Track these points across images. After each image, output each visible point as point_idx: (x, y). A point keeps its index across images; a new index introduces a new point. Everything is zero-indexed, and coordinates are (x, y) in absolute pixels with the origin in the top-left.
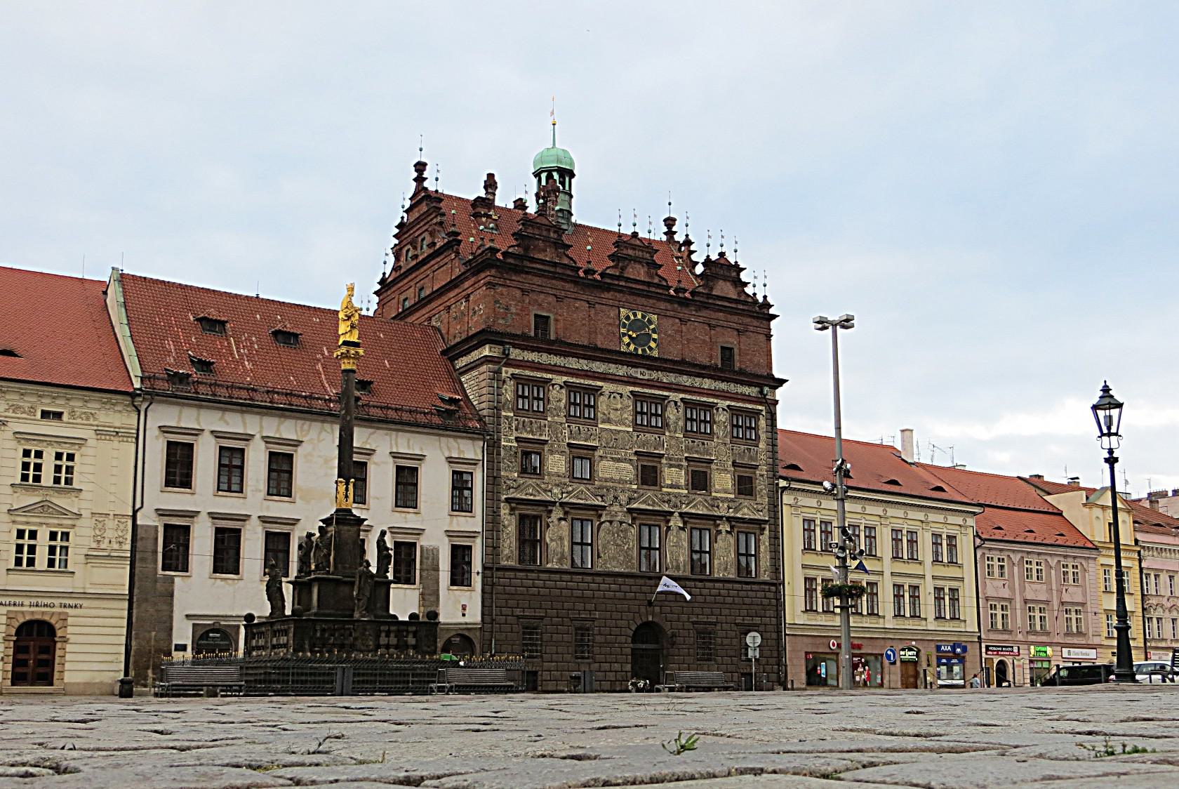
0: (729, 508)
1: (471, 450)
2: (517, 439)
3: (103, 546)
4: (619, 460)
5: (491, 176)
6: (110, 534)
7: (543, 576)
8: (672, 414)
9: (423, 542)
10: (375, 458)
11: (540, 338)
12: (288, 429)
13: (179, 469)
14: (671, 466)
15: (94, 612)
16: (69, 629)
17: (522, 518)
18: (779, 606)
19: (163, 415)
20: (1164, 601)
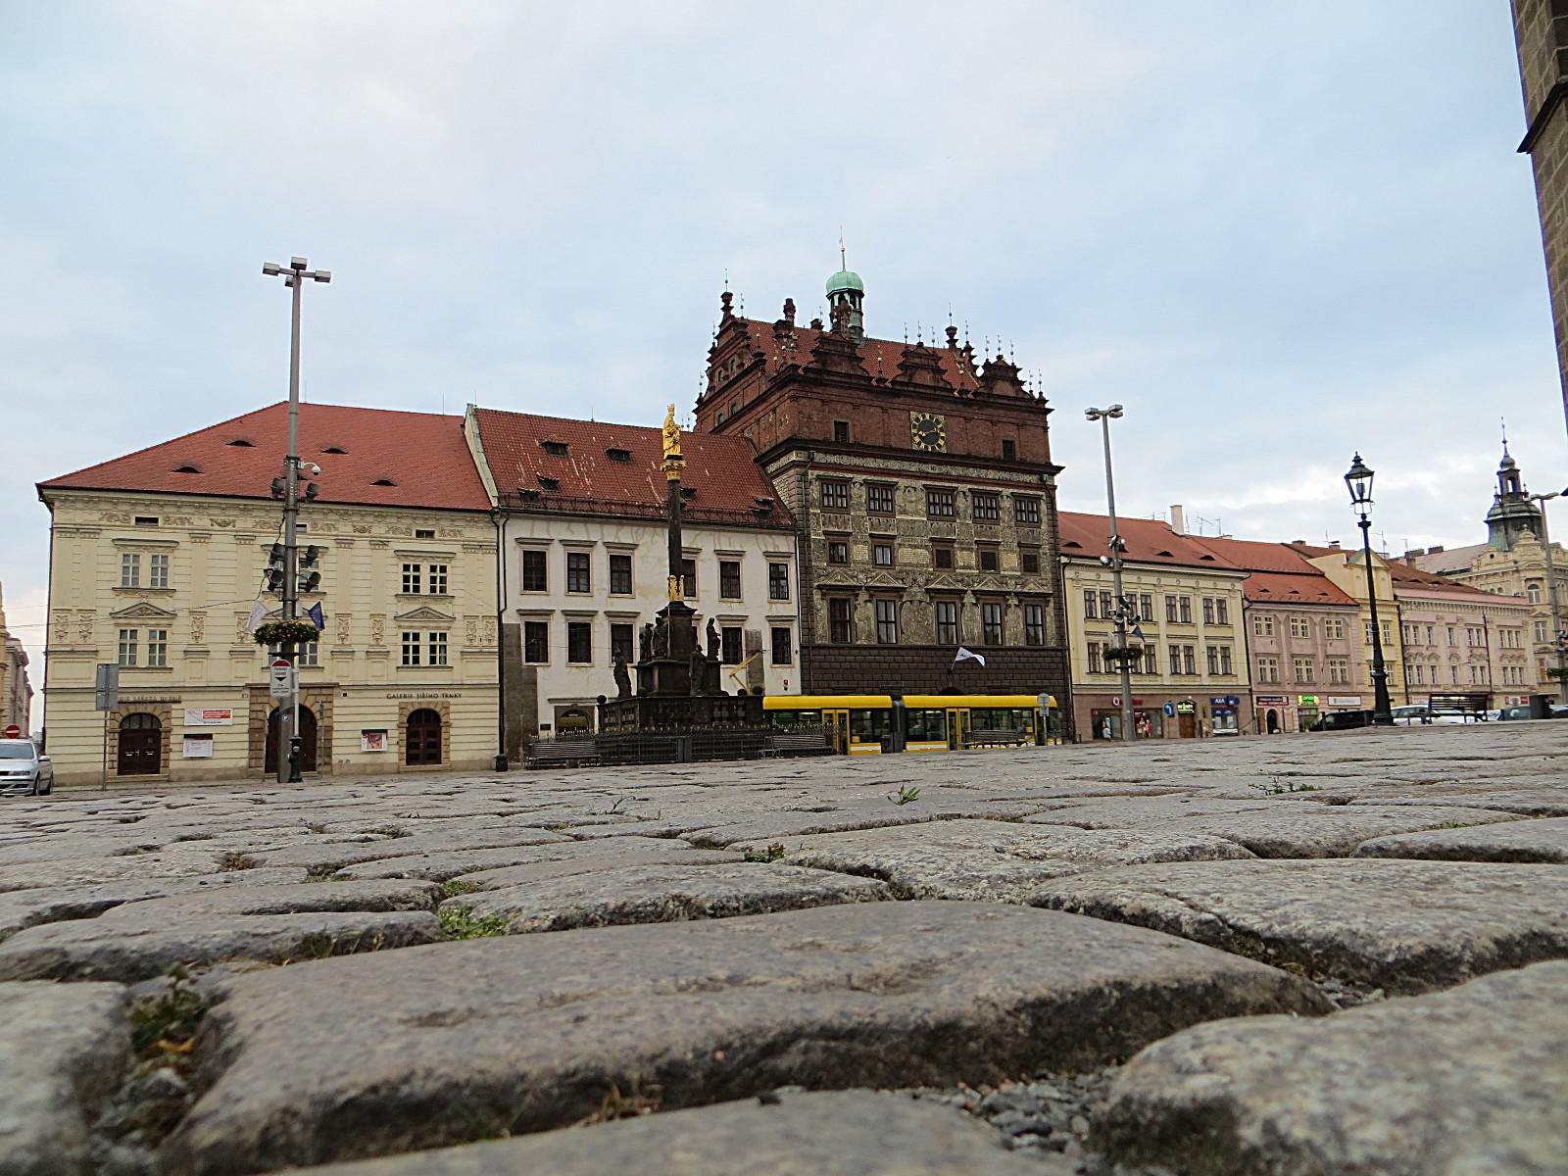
0: (1017, 584)
1: (785, 544)
2: (825, 533)
3: (475, 644)
4: (916, 547)
5: (789, 301)
6: (479, 633)
7: (853, 652)
8: (962, 503)
9: (747, 627)
10: (701, 556)
11: (841, 442)
12: (625, 535)
13: (535, 575)
14: (962, 549)
15: (471, 700)
16: (452, 716)
17: (833, 602)
18: (1065, 669)
19: (519, 529)
20: (1423, 650)
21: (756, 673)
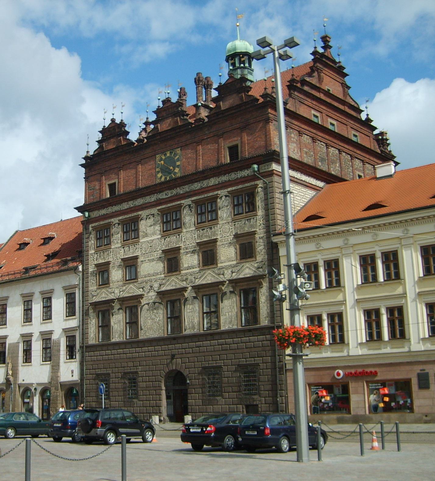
0: (232, 272)
14: (187, 253)
21: (55, 369)
